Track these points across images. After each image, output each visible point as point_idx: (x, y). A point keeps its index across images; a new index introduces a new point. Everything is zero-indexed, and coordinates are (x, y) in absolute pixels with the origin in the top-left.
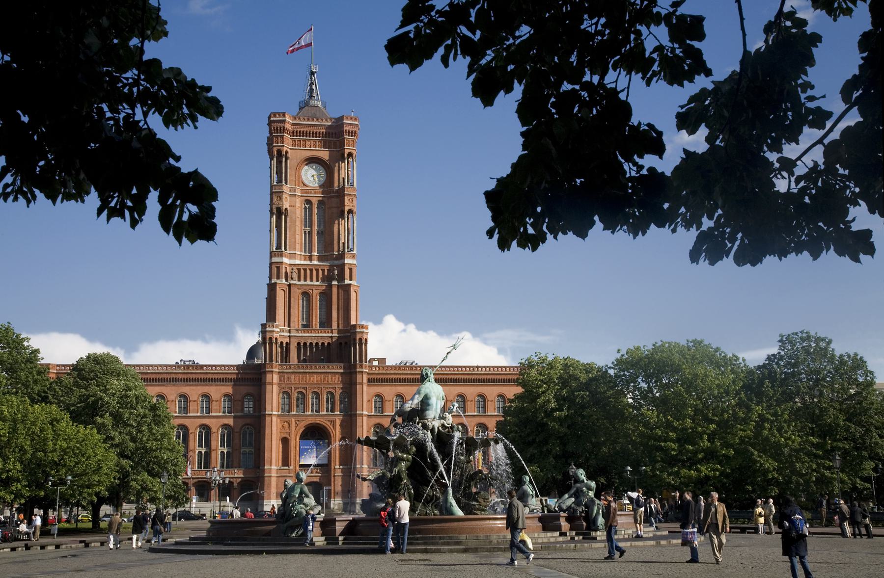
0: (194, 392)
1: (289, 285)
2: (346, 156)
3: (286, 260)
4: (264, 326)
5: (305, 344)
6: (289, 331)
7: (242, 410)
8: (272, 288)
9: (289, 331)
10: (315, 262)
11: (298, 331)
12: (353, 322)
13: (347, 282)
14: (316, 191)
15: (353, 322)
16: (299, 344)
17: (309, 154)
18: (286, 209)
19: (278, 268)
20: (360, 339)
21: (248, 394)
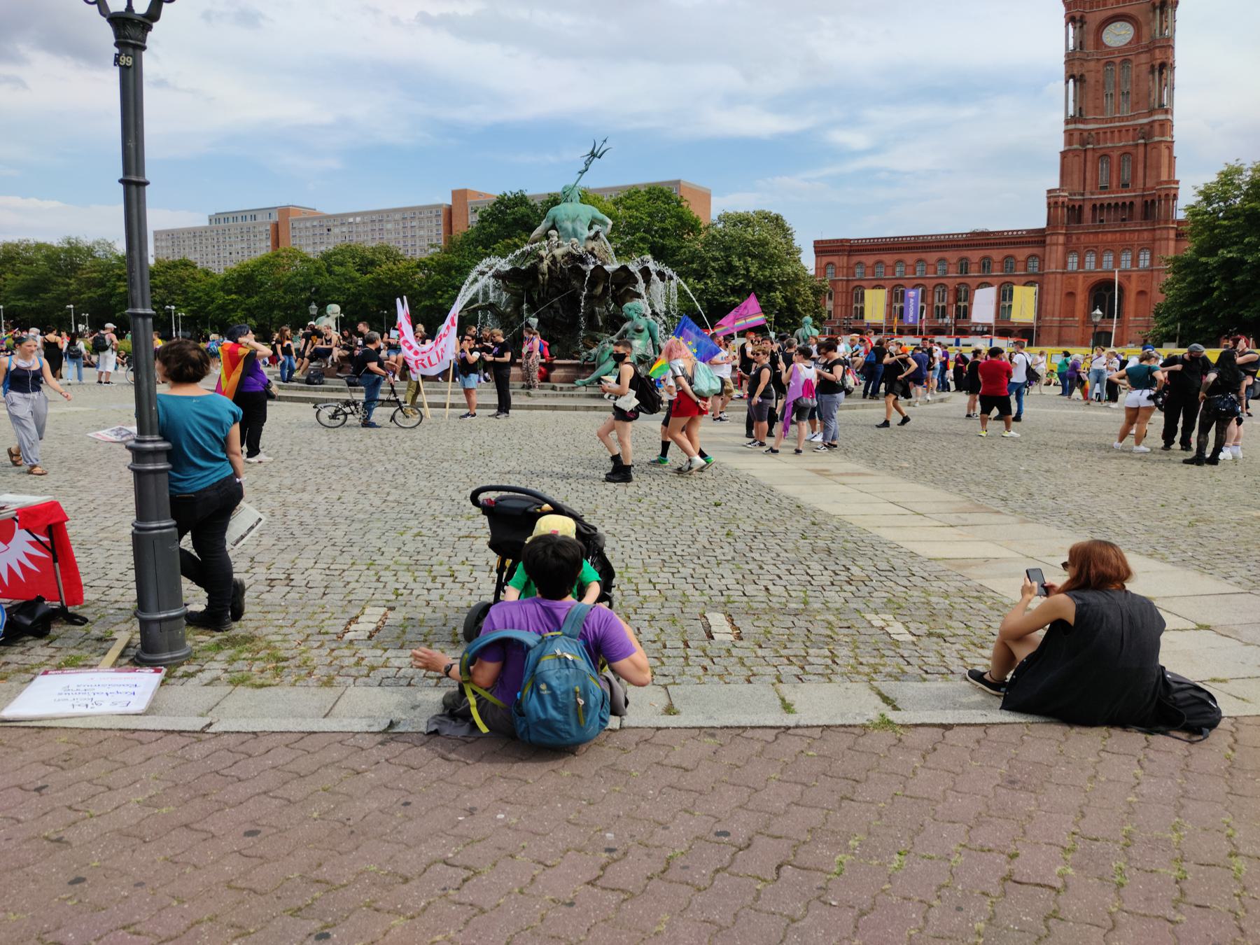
0: (975, 256)
2: (1158, 4)
3: (1081, 126)
5: (1102, 205)
6: (1083, 194)
7: (1026, 270)
8: (1064, 155)
9: (1083, 194)
11: (1092, 194)
12: (1164, 177)
13: (1156, 139)
14: (1120, 50)
15: (1164, 177)
16: (1094, 206)
17: (1110, 13)
18: (1082, 76)
20: (1167, 195)
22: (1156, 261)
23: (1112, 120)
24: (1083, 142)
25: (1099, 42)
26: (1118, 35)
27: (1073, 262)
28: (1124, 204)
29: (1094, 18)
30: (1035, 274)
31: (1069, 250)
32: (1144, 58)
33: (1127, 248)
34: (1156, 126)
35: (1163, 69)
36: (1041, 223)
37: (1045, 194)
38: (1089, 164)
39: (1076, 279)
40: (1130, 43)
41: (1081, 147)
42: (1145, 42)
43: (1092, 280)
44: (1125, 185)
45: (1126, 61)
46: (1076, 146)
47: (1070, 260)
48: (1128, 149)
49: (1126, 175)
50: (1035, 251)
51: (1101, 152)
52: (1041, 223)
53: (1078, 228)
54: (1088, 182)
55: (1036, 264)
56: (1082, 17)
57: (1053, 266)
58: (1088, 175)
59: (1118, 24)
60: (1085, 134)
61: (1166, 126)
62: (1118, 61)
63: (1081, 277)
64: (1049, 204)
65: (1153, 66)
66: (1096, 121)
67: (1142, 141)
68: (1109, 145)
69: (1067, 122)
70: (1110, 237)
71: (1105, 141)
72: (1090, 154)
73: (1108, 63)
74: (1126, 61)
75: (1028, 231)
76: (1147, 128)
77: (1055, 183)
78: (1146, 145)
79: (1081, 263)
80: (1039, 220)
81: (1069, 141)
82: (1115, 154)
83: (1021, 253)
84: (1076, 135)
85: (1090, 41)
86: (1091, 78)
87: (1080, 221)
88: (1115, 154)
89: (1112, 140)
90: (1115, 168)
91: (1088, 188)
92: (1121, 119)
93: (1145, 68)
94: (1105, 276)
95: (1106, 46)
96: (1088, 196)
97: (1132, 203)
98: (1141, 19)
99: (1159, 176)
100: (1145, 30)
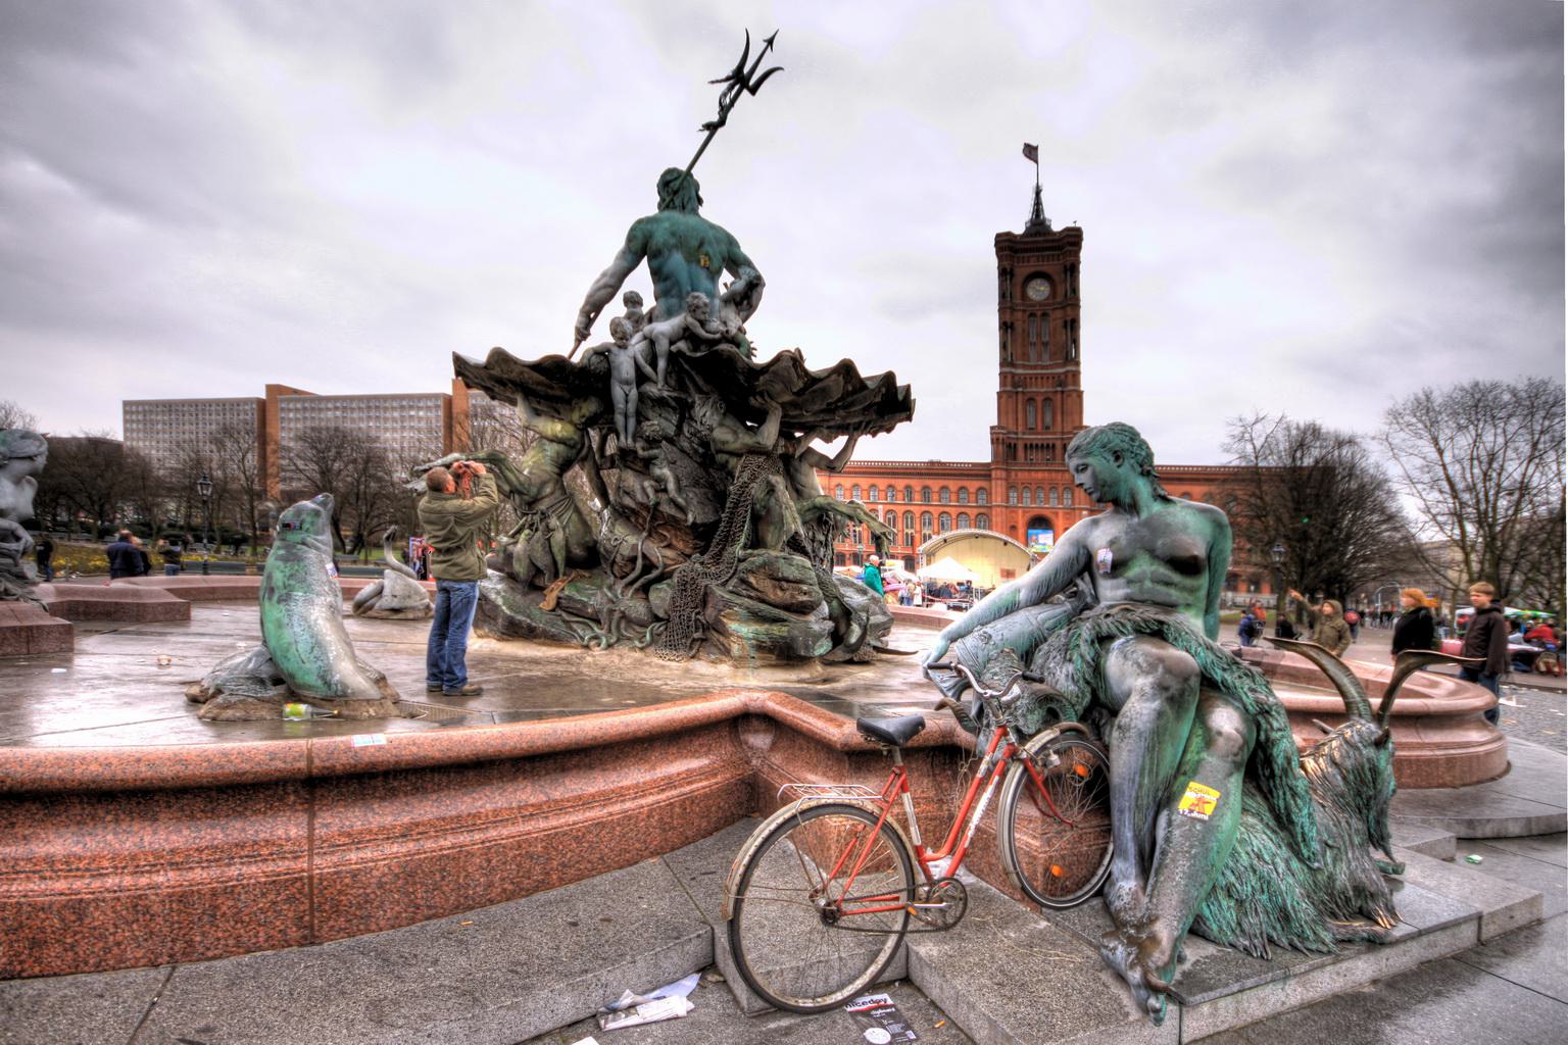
1: (1017, 393)
4: (992, 428)
6: (1016, 433)
9: (1016, 433)
10: (1039, 371)
11: (1024, 433)
13: (1071, 388)
14: (1040, 304)
15: (1077, 424)
16: (1026, 445)
17: (1033, 270)
18: (1012, 324)
19: (1005, 377)
21: (981, 488)
22: (1077, 501)
23: (1035, 367)
24: (1015, 385)
25: (1024, 296)
26: (1039, 291)
27: (1013, 495)
28: (1048, 445)
29: (1022, 271)
30: (984, 507)
31: (1011, 487)
32: (1059, 314)
33: (1053, 488)
34: (1070, 375)
35: (1072, 325)
36: (988, 459)
37: (988, 431)
38: (1020, 407)
39: (1016, 512)
40: (1048, 298)
41: (1014, 390)
42: (1059, 299)
43: (1029, 516)
44: (1048, 428)
45: (1044, 315)
46: (1009, 388)
47: (1011, 494)
48: (1051, 396)
49: (1048, 419)
50: (984, 484)
51: (1029, 396)
52: (988, 459)
53: (1016, 465)
54: (1020, 422)
55: (985, 496)
56: (1012, 270)
57: (999, 499)
58: (1020, 416)
59: (1039, 281)
60: (1016, 378)
61: (1076, 375)
62: (1039, 313)
63: (1020, 511)
64: (992, 440)
65: (1066, 322)
66: (1024, 367)
67: (1059, 389)
68: (1034, 389)
69: (1002, 365)
70: (1040, 475)
71: (1031, 386)
72: (1020, 396)
73: (1032, 315)
74: (1044, 315)
75: (974, 464)
76: (1063, 377)
77: (996, 423)
78: (1062, 392)
79: (1020, 499)
80: (983, 453)
81: (1003, 383)
82: (1039, 399)
83: (973, 485)
84: (1009, 376)
85: (1018, 294)
86: (1019, 326)
87: (1015, 458)
88: (1039, 399)
89: (1036, 385)
90: (1040, 411)
91: (1020, 429)
92: (1043, 367)
93: (1060, 323)
94: (1037, 512)
95: (1030, 300)
96: (1020, 436)
97: (1054, 445)
98: (1056, 278)
99: (1073, 422)
100: (1060, 290)
